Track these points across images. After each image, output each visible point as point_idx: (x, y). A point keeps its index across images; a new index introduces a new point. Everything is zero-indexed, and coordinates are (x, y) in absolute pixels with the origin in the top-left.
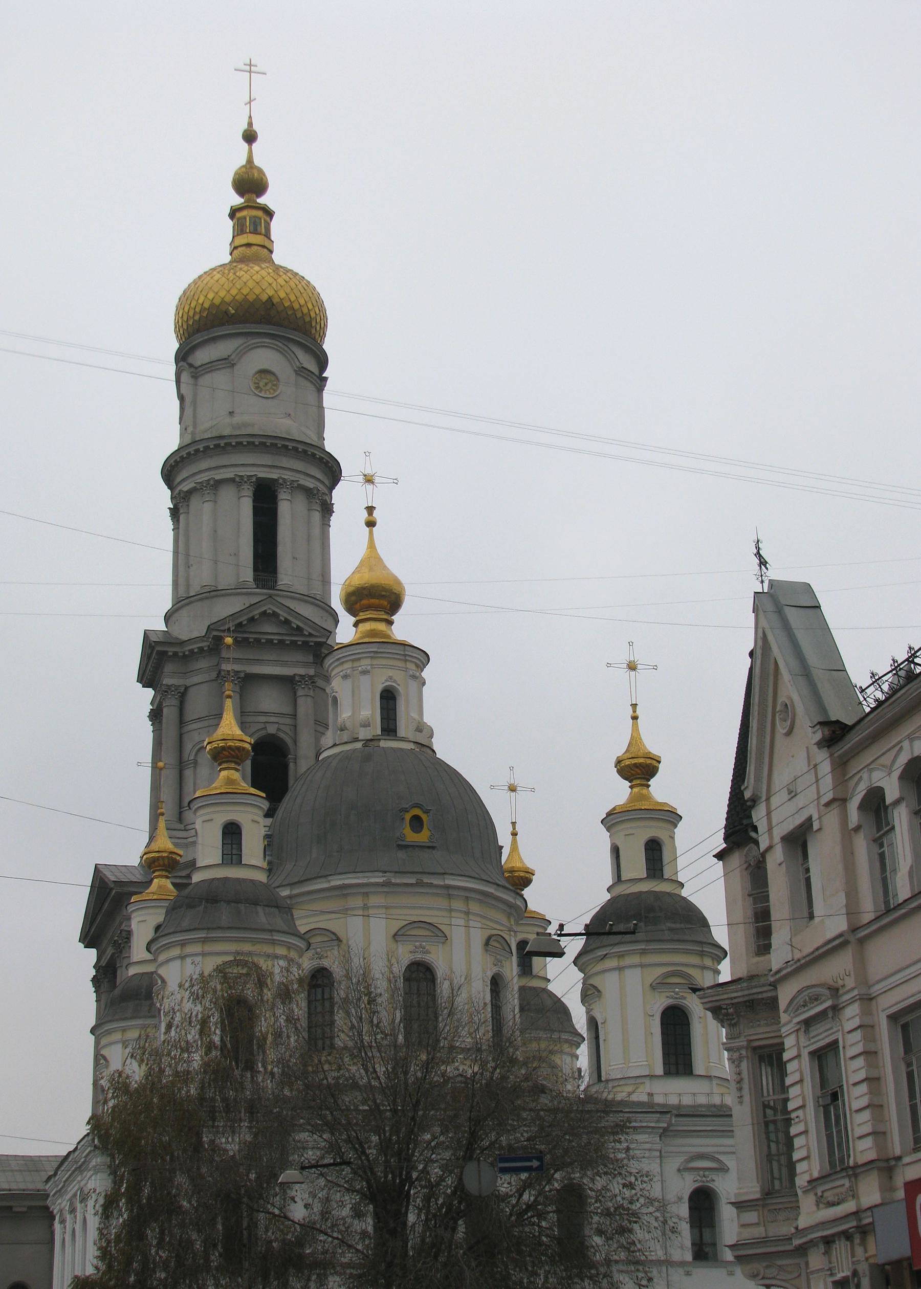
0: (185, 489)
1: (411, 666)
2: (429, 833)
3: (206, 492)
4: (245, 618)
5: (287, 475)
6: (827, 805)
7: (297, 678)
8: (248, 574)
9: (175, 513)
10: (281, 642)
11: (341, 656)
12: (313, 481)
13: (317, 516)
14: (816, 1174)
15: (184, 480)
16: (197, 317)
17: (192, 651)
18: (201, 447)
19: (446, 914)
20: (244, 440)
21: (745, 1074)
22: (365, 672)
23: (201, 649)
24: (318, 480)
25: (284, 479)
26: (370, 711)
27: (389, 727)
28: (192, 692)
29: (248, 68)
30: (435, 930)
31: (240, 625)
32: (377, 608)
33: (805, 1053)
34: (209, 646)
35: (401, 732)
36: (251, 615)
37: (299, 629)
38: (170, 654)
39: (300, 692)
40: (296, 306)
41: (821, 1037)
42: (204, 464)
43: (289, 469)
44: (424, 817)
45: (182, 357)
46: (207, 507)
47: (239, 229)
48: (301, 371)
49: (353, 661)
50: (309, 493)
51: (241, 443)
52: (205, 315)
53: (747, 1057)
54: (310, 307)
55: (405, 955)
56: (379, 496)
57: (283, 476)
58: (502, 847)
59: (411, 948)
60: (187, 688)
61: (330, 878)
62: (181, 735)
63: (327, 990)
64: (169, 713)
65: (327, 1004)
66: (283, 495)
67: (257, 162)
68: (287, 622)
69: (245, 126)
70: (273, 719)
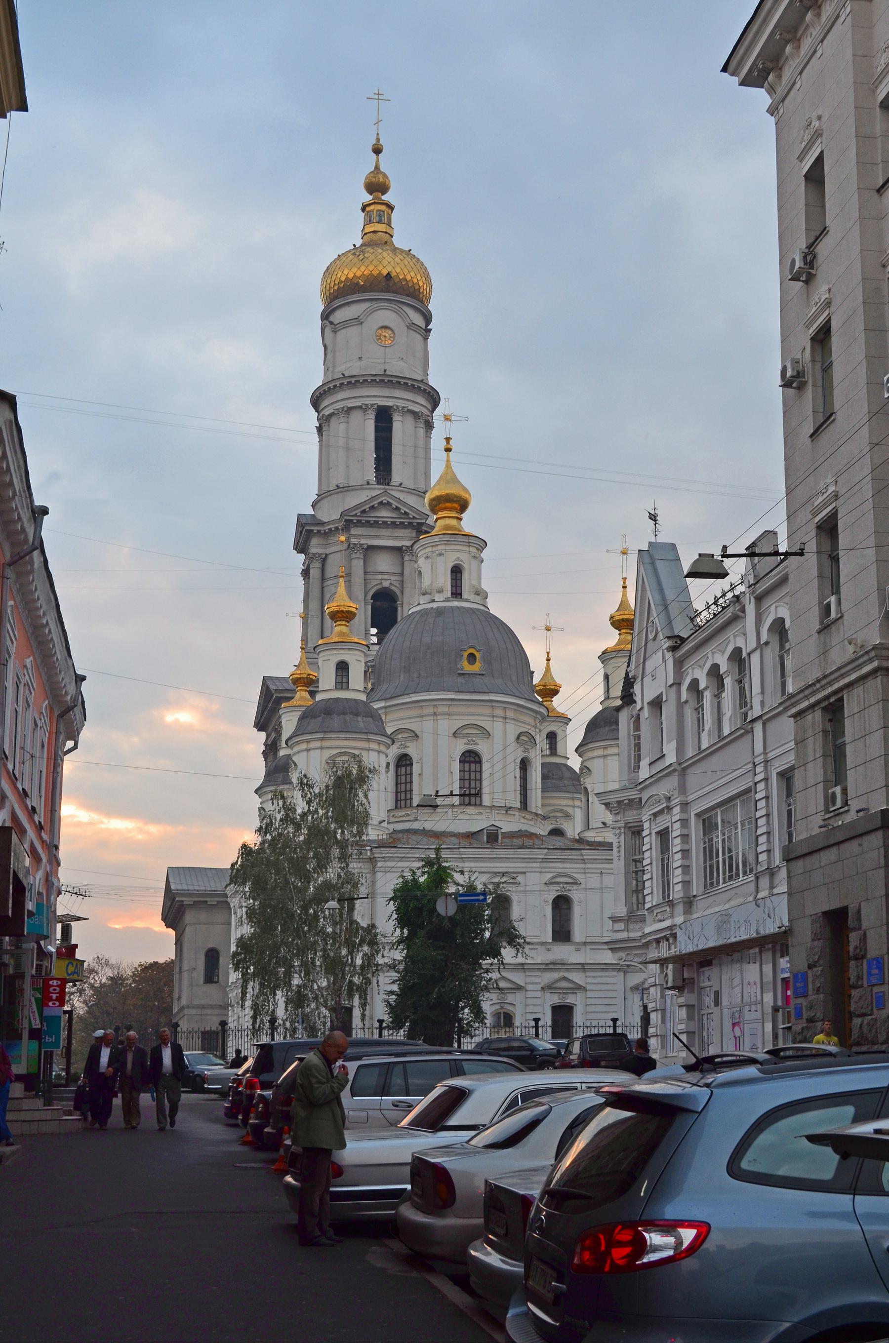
0: (327, 413)
1: (473, 550)
2: (480, 665)
4: (368, 506)
5: (400, 403)
6: (671, 686)
8: (371, 476)
9: (320, 429)
10: (394, 523)
12: (419, 406)
13: (421, 432)
14: (654, 904)
15: (325, 407)
16: (336, 288)
17: (330, 529)
18: (338, 384)
19: (491, 719)
20: (369, 379)
21: (622, 844)
22: (440, 555)
23: (337, 528)
24: (422, 405)
25: (397, 407)
26: (445, 581)
27: (457, 593)
28: (331, 559)
29: (376, 97)
30: (482, 729)
31: (364, 511)
32: (451, 509)
33: (653, 832)
35: (465, 595)
36: (371, 504)
37: (406, 513)
38: (315, 531)
39: (406, 558)
40: (408, 278)
41: (662, 822)
42: (341, 395)
43: (402, 399)
44: (477, 654)
45: (326, 316)
46: (342, 427)
47: (368, 221)
48: (412, 326)
49: (432, 546)
50: (416, 415)
51: (366, 380)
52: (342, 286)
53: (625, 833)
54: (419, 278)
55: (461, 746)
56: (456, 431)
57: (397, 404)
58: (533, 672)
59: (465, 741)
60: (327, 555)
61: (411, 695)
62: (323, 588)
63: (408, 768)
64: (315, 572)
65: (408, 777)
66: (396, 418)
67: (382, 170)
68: (397, 509)
69: (374, 142)
70: (386, 577)
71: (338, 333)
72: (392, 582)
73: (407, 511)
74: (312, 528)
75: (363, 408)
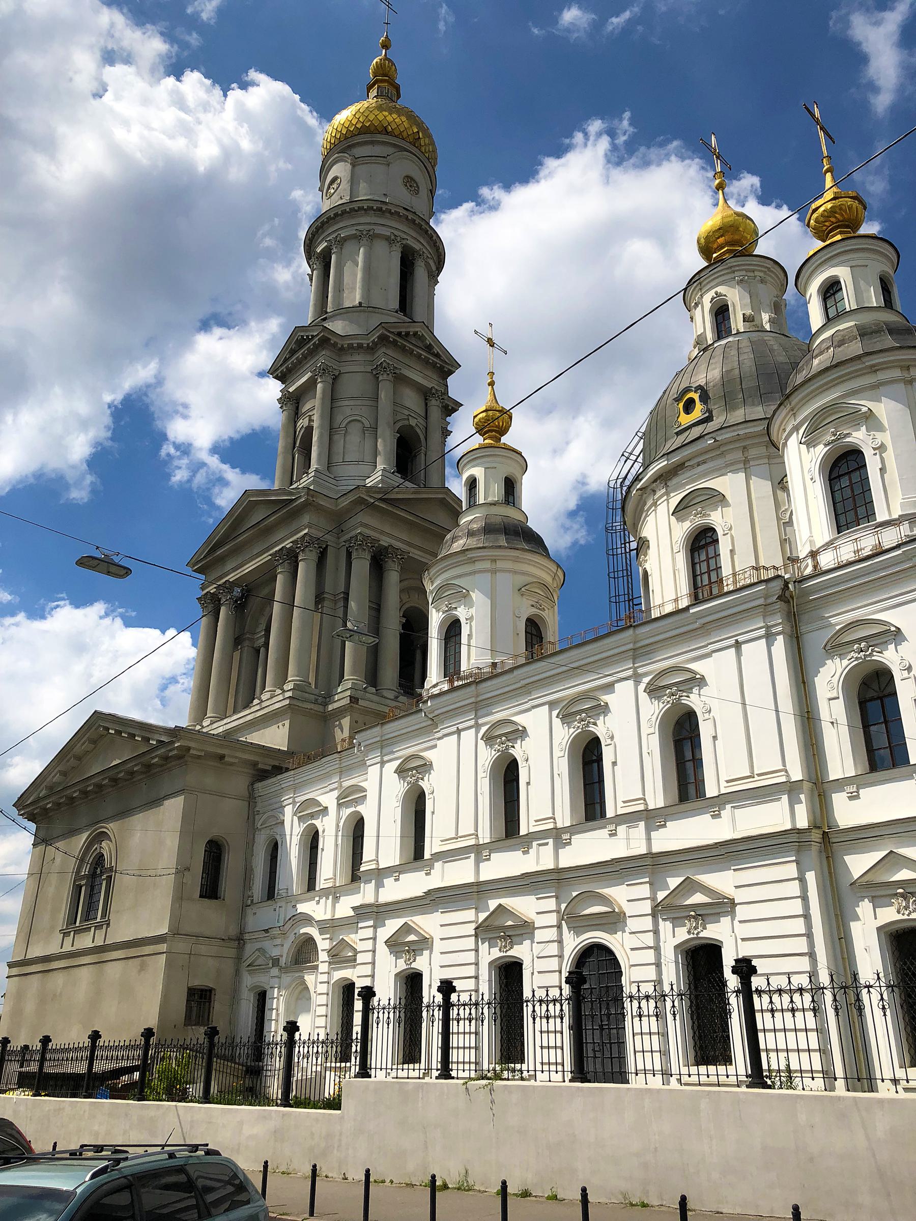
3: (364, 239)
7: (434, 391)
11: (735, 264)
16: (359, 126)
20: (402, 212)
23: (360, 346)
25: (423, 252)
28: (345, 379)
31: (399, 334)
34: (368, 344)
38: (332, 342)
71: (357, 168)
72: (418, 423)
73: (441, 353)
74: (330, 337)
75: (390, 240)
